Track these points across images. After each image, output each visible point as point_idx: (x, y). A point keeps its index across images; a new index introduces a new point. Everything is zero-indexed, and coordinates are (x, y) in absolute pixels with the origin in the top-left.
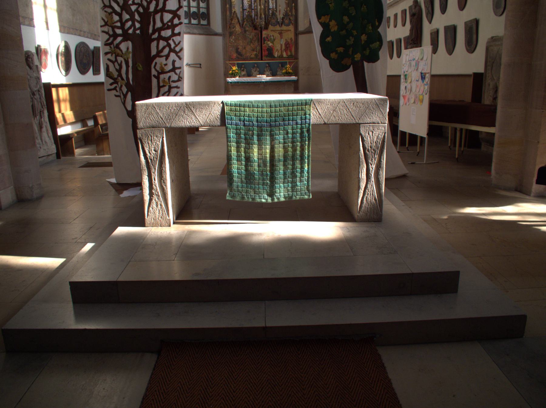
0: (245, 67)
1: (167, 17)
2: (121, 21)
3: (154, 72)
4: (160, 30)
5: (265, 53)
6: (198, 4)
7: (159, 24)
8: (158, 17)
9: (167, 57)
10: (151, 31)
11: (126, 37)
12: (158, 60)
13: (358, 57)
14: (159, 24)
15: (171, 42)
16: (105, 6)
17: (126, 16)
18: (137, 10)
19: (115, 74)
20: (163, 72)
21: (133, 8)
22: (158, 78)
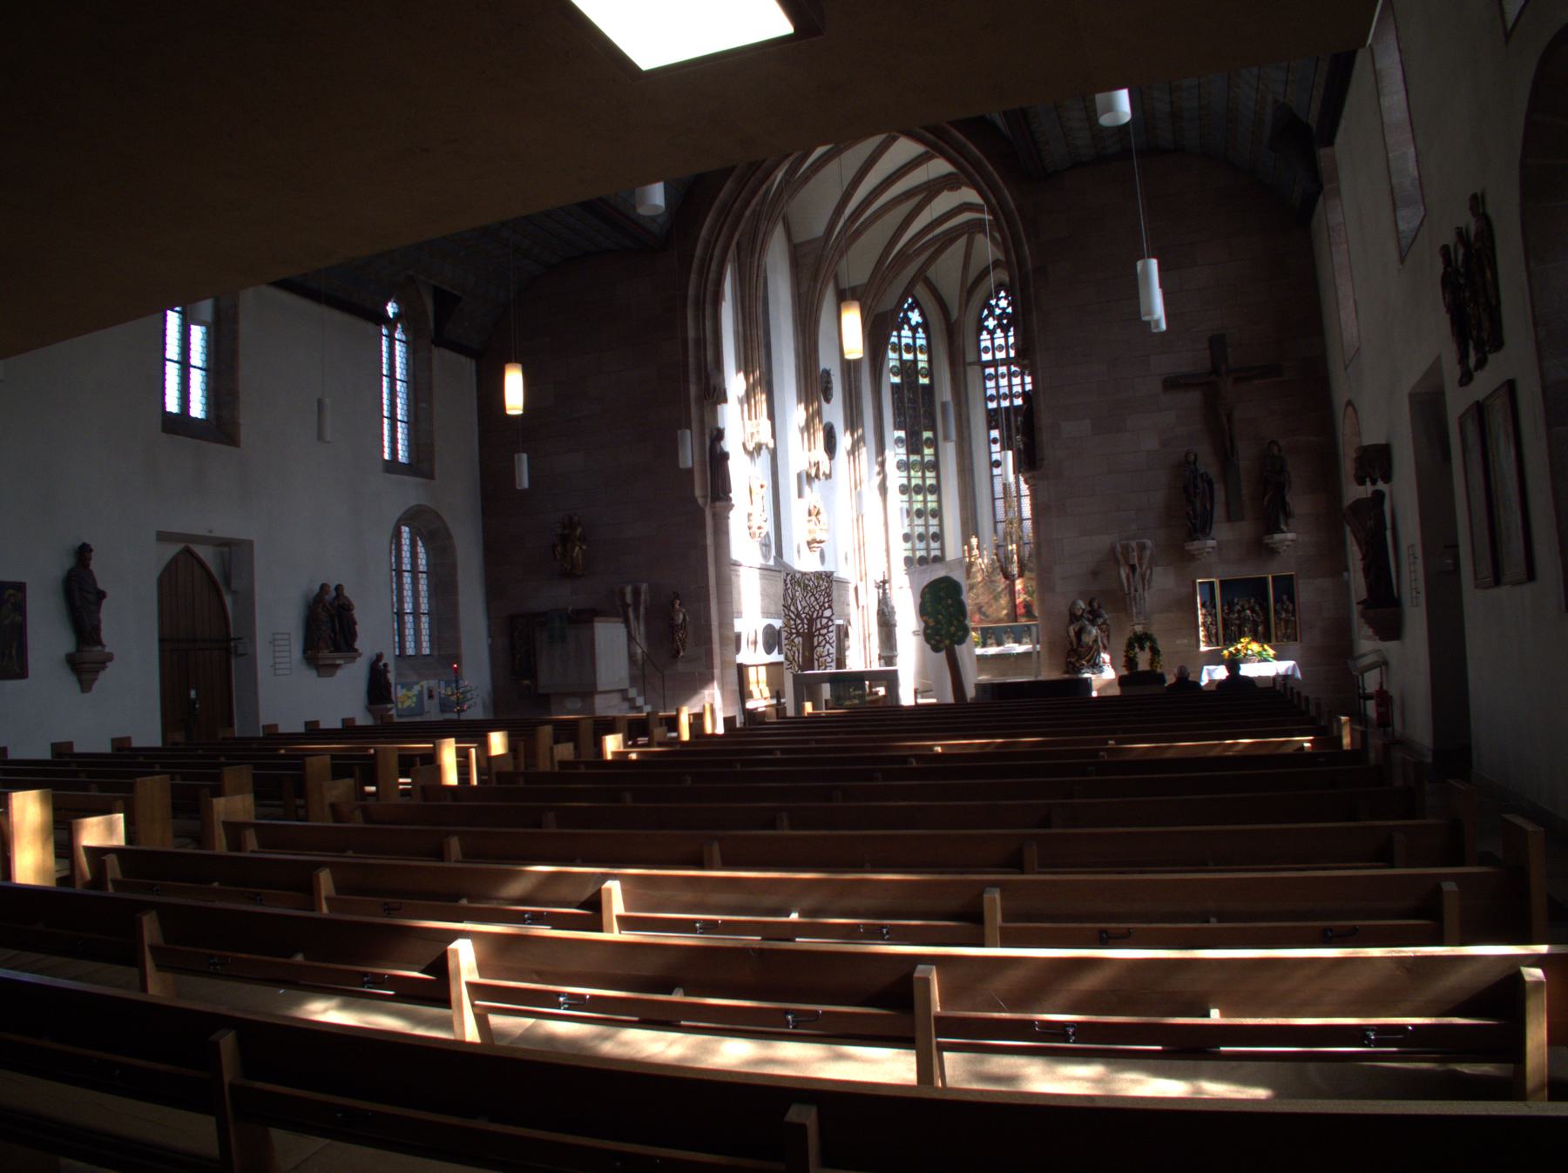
0: (993, 633)
1: (824, 621)
2: (795, 624)
3: (816, 657)
4: (819, 629)
5: (1021, 610)
6: (928, 545)
7: (819, 626)
8: (818, 621)
9: (824, 646)
10: (814, 630)
11: (798, 634)
12: (818, 649)
13: (947, 642)
14: (819, 626)
15: (827, 637)
16: (786, 615)
17: (799, 622)
18: (806, 617)
19: (791, 659)
20: (822, 657)
21: (803, 616)
22: (818, 660)
